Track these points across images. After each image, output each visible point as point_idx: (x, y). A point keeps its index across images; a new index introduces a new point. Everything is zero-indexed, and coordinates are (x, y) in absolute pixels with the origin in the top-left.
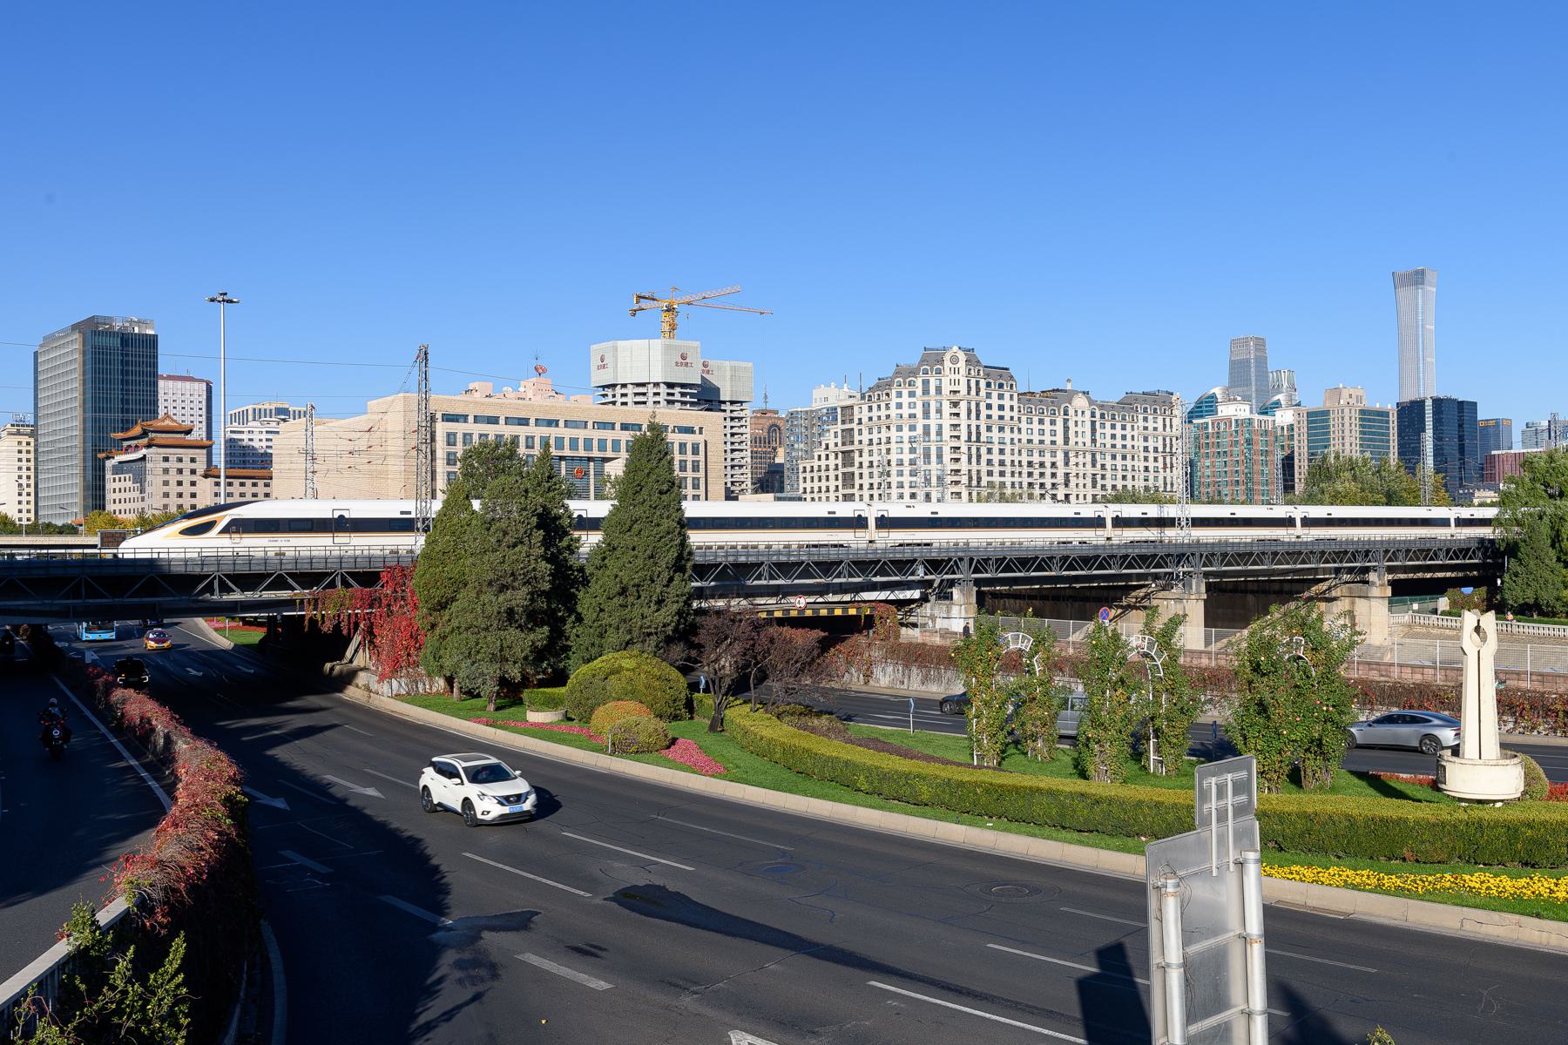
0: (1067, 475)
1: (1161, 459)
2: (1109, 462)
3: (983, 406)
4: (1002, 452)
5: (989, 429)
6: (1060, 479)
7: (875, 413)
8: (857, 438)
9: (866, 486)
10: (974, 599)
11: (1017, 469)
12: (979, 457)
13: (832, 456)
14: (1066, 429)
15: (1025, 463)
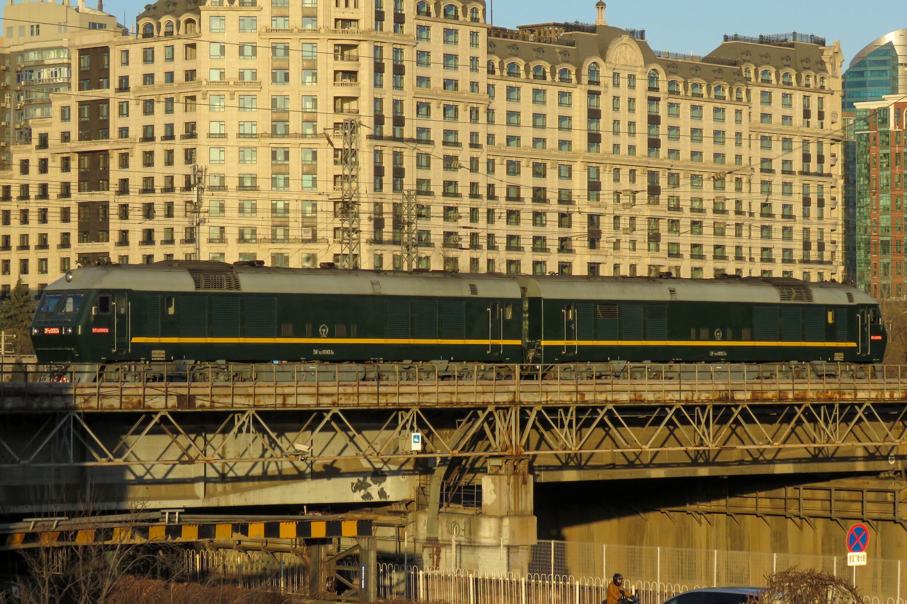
0: (593, 220)
1: (797, 188)
2: (685, 193)
3: (409, 55)
4: (450, 163)
5: (423, 108)
6: (579, 225)
7: (159, 69)
8: (115, 122)
9: (136, 237)
10: (528, 501)
11: (483, 206)
12: (399, 173)
13: (54, 166)
14: (594, 115)
15: (501, 192)
